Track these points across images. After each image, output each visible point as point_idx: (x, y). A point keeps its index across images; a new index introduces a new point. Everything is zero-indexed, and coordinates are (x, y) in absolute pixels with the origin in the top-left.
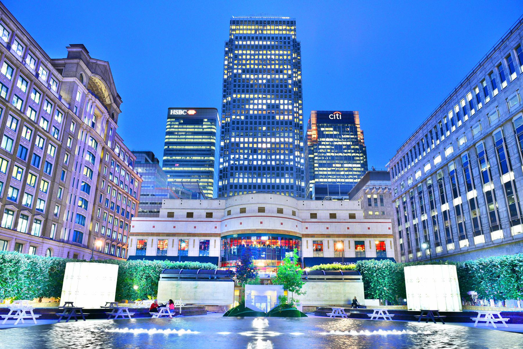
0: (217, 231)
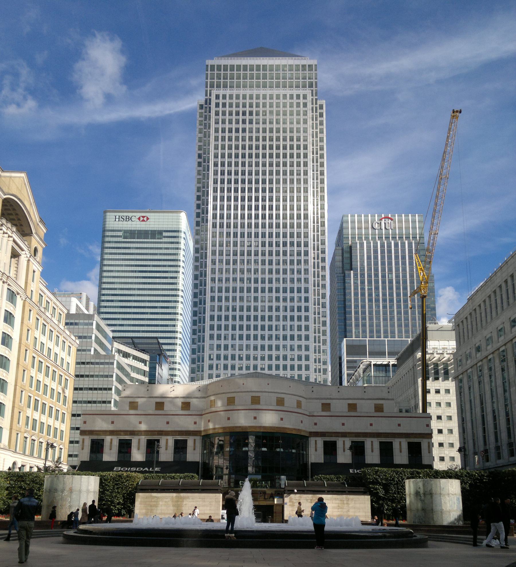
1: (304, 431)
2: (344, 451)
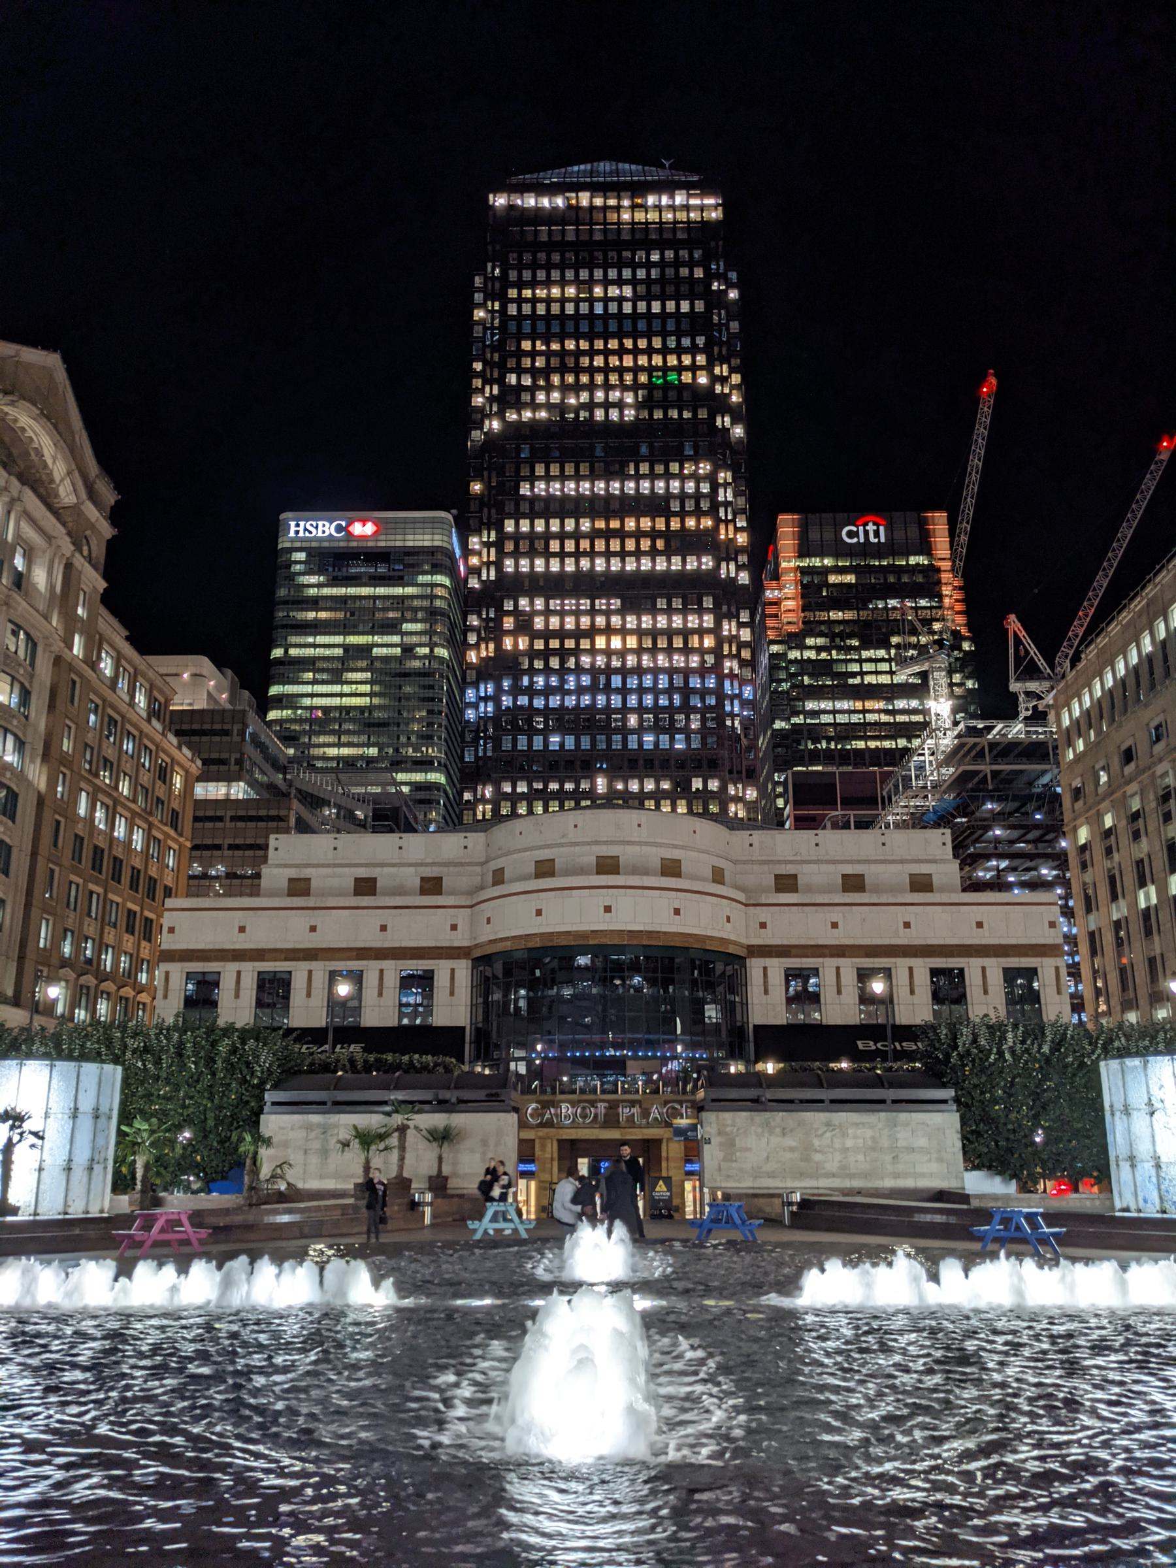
0: (461, 939)
1: (735, 943)
2: (839, 992)
